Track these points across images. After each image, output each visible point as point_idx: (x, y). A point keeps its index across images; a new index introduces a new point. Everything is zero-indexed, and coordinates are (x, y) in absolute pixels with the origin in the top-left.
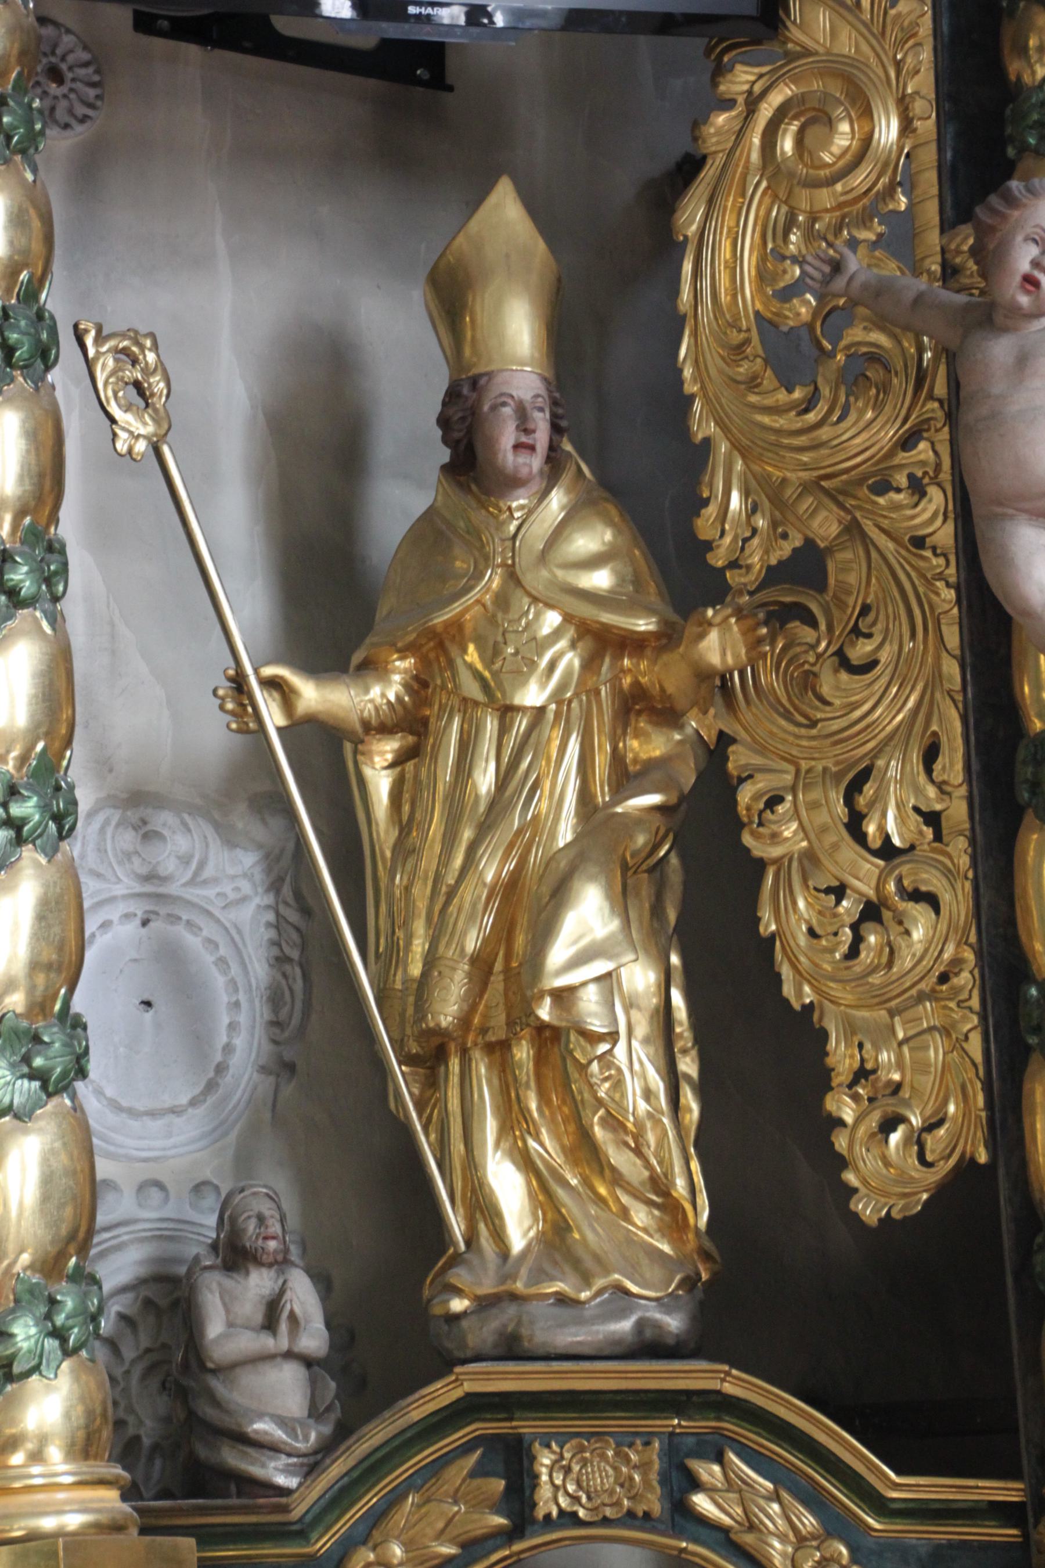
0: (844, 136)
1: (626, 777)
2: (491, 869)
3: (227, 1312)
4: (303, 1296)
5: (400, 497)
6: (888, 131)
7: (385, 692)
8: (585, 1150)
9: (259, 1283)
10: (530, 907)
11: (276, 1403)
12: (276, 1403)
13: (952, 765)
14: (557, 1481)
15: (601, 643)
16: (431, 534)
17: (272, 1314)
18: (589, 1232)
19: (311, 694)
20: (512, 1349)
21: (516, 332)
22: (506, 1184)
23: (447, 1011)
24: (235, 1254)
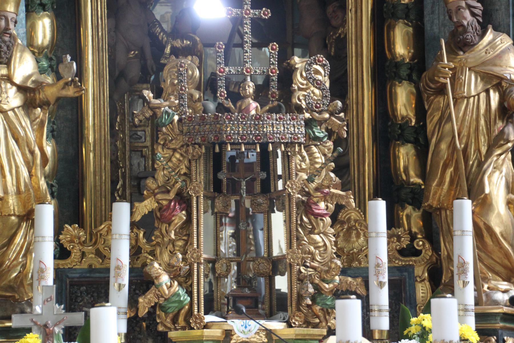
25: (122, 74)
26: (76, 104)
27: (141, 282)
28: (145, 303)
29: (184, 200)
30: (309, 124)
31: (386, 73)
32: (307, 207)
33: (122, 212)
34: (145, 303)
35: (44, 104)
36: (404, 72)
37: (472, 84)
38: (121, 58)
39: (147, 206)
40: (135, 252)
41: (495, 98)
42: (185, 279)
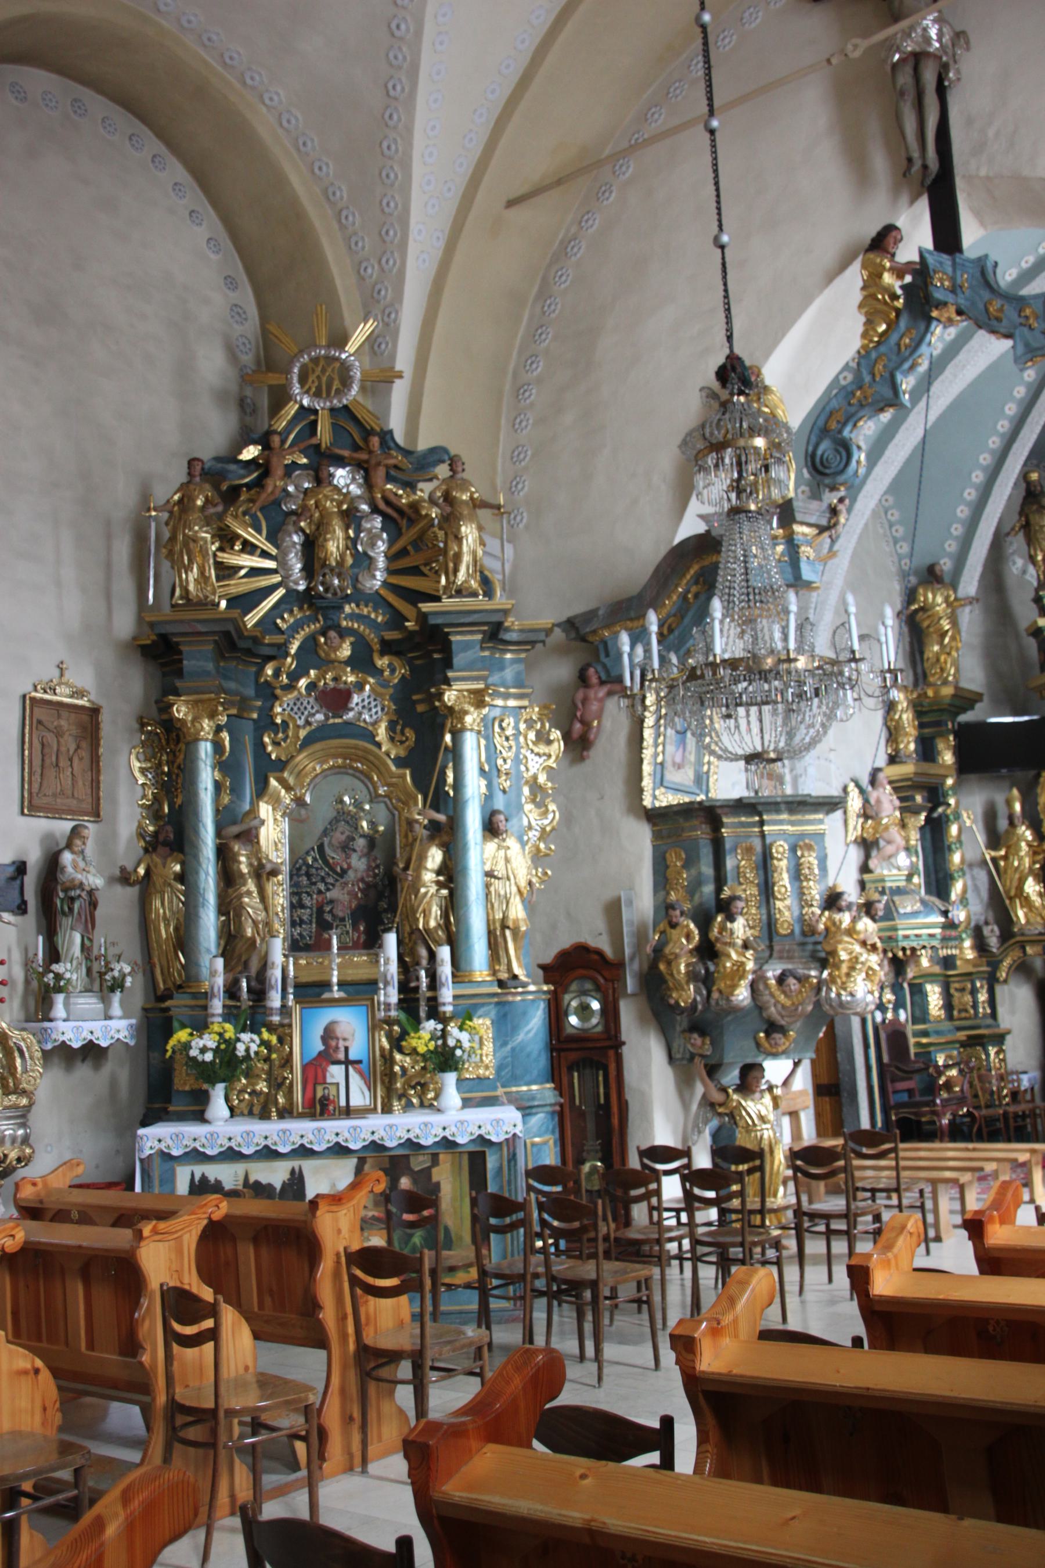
1: (1034, 863)
2: (1017, 876)
3: (986, 931)
4: (996, 928)
5: (1003, 824)
7: (1003, 853)
8: (1031, 910)
9: (990, 927)
10: (1022, 881)
11: (993, 942)
12: (993, 942)
14: (1029, 950)
15: (1029, 845)
16: (1007, 832)
17: (992, 931)
18: (1032, 920)
19: (993, 853)
20: (1023, 935)
21: (1018, 807)
22: (1021, 914)
23: (1012, 893)
24: (987, 923)
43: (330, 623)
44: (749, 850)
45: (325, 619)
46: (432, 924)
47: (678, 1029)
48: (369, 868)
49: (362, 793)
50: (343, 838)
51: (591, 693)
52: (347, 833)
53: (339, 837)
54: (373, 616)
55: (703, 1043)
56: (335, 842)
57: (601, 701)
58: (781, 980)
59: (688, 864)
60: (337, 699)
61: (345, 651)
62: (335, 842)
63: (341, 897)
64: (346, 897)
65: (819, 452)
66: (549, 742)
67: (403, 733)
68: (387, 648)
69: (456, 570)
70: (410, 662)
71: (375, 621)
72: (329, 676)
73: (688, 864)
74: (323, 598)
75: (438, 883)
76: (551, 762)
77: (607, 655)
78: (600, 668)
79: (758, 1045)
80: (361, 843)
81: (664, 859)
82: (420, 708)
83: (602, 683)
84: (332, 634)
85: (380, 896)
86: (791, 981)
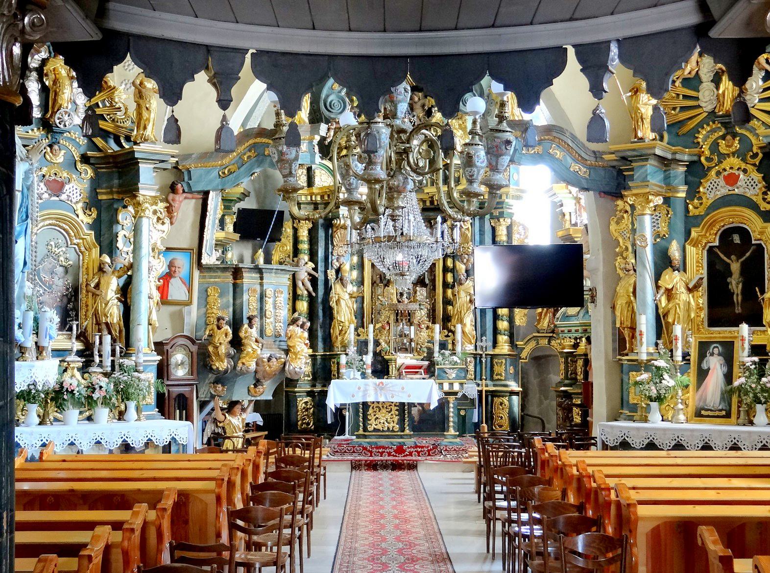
0: (285, 248)
6: (288, 248)
13: (291, 295)
25: (375, 282)
26: (363, 297)
27: (377, 343)
28: (378, 349)
29: (388, 323)
30: (420, 305)
31: (446, 285)
32: (419, 325)
33: (371, 327)
34: (378, 349)
35: (354, 297)
36: (450, 286)
37: (462, 294)
38: (375, 278)
39: (378, 326)
40: (375, 336)
41: (468, 298)
42: (388, 343)
43: (54, 140)
44: (255, 291)
45: (52, 138)
46: (115, 321)
47: (207, 381)
48: (65, 285)
49: (61, 241)
50: (50, 266)
51: (177, 197)
52: (53, 264)
53: (47, 265)
54: (77, 140)
55: (223, 390)
56: (46, 269)
57: (181, 202)
58: (269, 360)
59: (221, 295)
60: (57, 187)
61: (60, 159)
62: (46, 269)
63: (48, 300)
64: (51, 301)
65: (329, 100)
66: (163, 223)
67: (91, 211)
68: (85, 159)
69: (145, 128)
70: (95, 171)
71: (78, 143)
72: (53, 171)
73: (221, 295)
74: (58, 127)
75: (117, 298)
76: (164, 235)
77: (190, 179)
78: (185, 185)
79: (249, 391)
80: (60, 270)
81: (206, 291)
82: (104, 197)
83: (184, 192)
84: (56, 147)
85: (69, 301)
86: (274, 360)
